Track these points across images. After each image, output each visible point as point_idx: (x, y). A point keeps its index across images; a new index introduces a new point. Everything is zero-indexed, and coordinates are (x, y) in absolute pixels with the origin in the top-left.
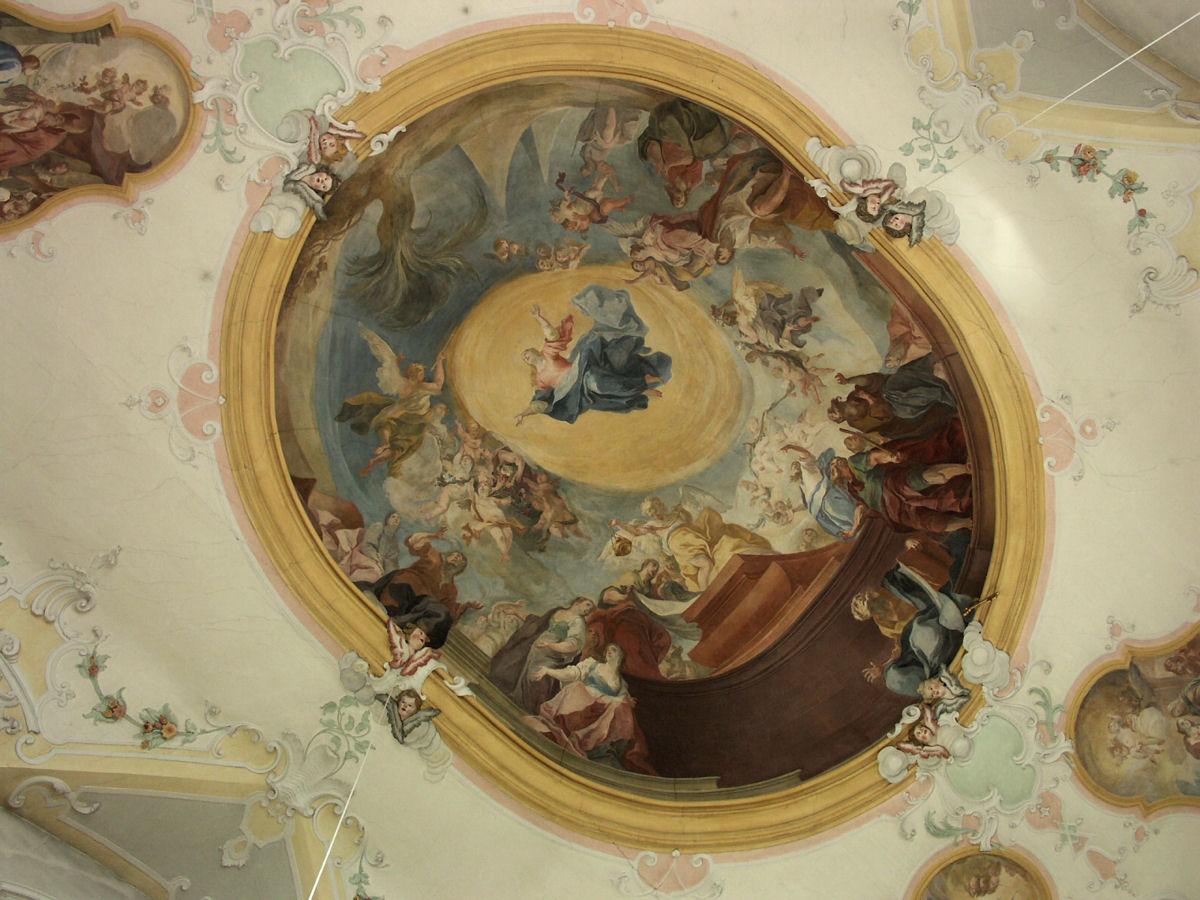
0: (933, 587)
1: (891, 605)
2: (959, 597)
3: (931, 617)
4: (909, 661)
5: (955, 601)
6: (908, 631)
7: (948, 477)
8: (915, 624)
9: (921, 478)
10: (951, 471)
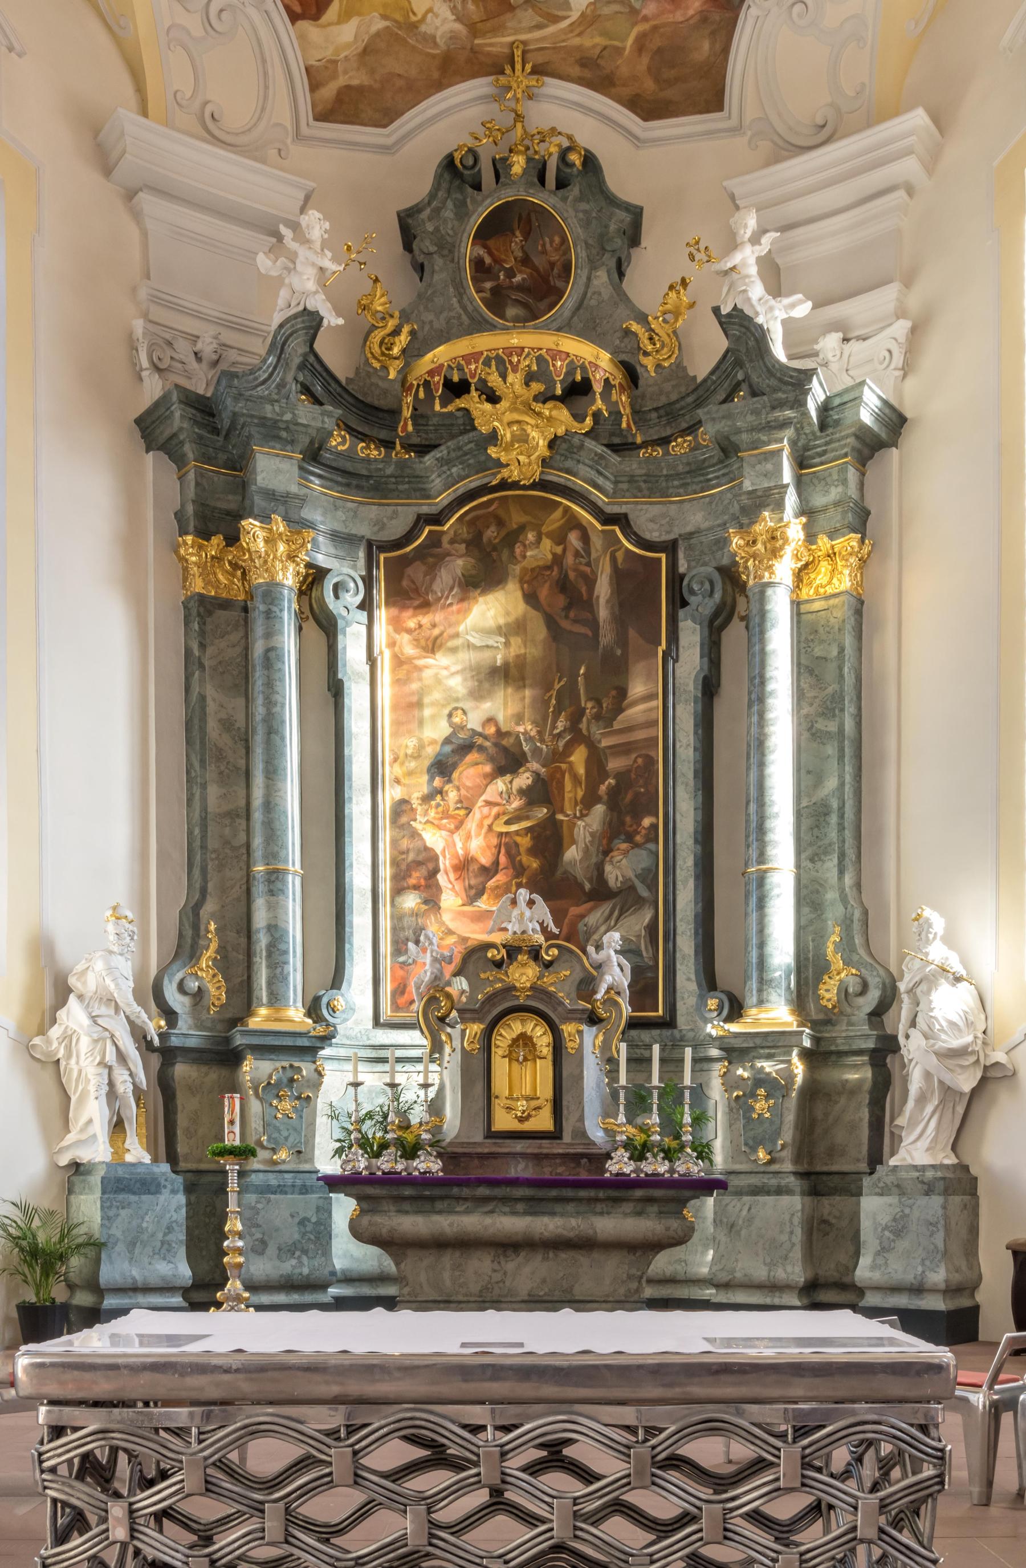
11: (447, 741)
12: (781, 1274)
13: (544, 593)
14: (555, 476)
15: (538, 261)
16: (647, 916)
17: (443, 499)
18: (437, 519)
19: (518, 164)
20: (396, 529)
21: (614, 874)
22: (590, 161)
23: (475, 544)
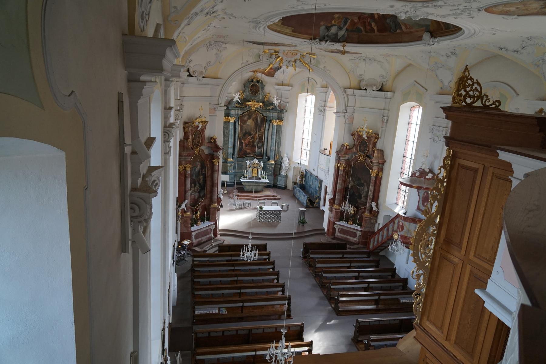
0: (347, 27)
1: (340, 20)
2: (346, 34)
3: (340, 29)
4: (328, 28)
5: (345, 33)
6: (335, 25)
7: (374, 28)
8: (337, 26)
9: (373, 22)
10: (375, 28)
11: (245, 133)
12: (271, 183)
13: (255, 120)
14: (256, 109)
15: (256, 89)
16: (261, 149)
17: (246, 111)
18: (245, 112)
19: (255, 80)
20: (241, 113)
21: (259, 145)
22: (262, 81)
23: (249, 115)
